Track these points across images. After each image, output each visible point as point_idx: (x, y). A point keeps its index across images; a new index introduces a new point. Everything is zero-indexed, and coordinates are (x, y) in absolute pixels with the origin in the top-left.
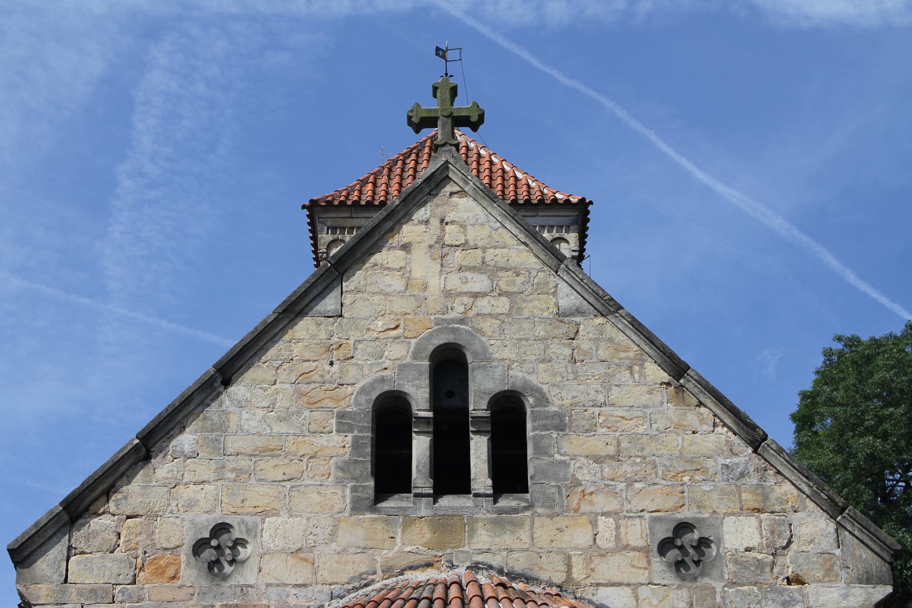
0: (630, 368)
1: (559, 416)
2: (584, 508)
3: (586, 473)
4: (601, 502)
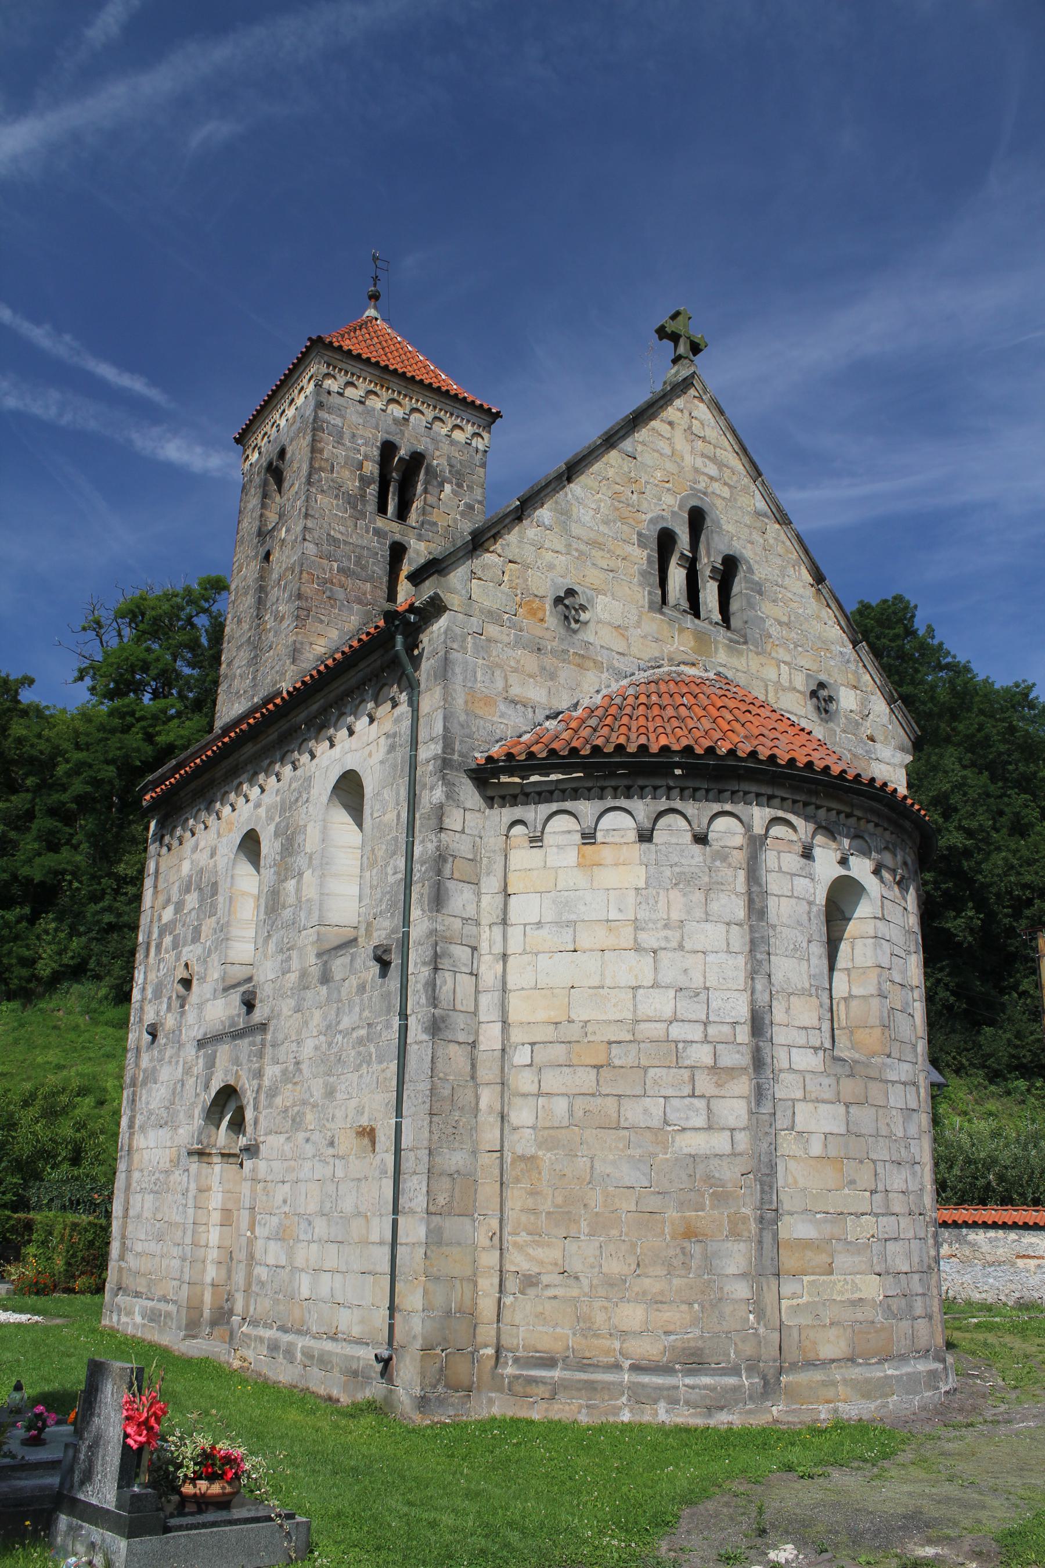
0: (794, 566)
2: (774, 654)
3: (774, 630)
4: (782, 654)
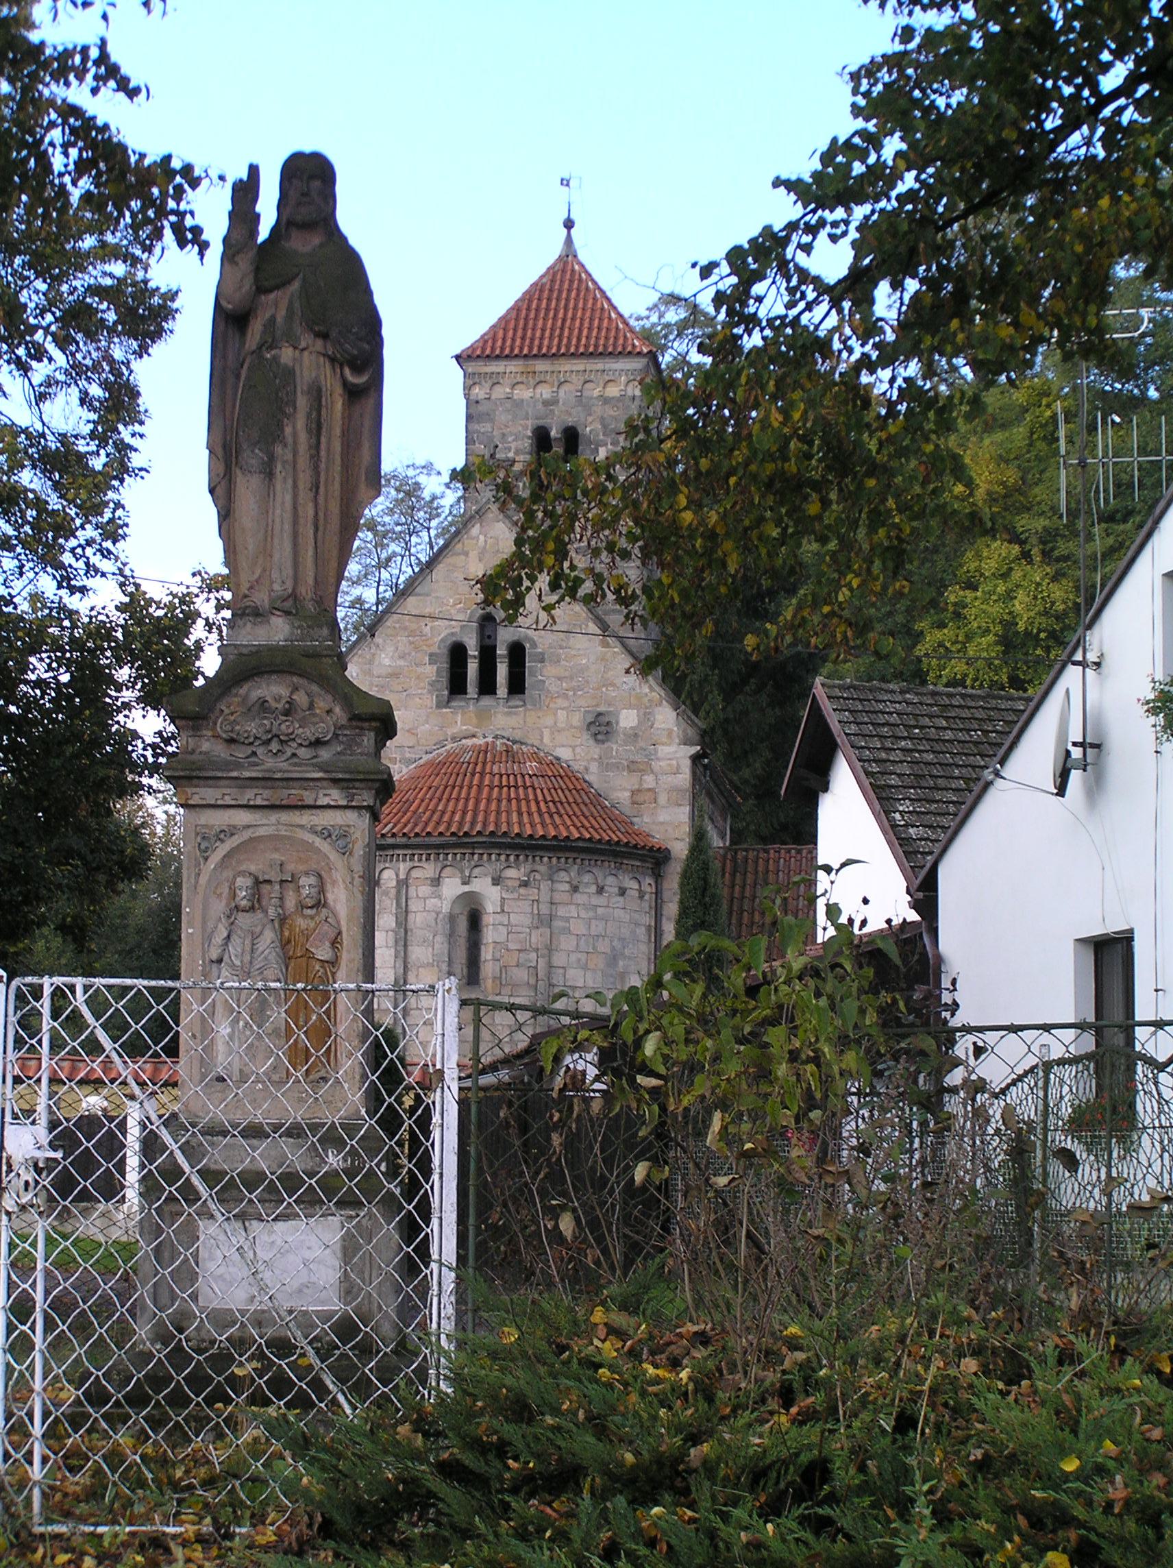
1: (542, 654)
3: (553, 686)
